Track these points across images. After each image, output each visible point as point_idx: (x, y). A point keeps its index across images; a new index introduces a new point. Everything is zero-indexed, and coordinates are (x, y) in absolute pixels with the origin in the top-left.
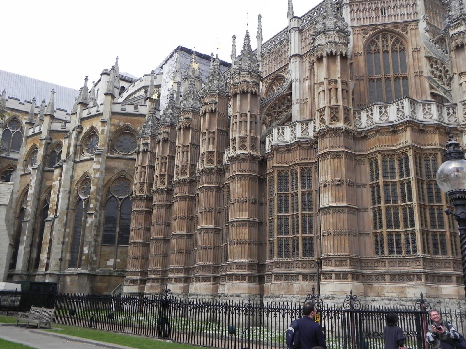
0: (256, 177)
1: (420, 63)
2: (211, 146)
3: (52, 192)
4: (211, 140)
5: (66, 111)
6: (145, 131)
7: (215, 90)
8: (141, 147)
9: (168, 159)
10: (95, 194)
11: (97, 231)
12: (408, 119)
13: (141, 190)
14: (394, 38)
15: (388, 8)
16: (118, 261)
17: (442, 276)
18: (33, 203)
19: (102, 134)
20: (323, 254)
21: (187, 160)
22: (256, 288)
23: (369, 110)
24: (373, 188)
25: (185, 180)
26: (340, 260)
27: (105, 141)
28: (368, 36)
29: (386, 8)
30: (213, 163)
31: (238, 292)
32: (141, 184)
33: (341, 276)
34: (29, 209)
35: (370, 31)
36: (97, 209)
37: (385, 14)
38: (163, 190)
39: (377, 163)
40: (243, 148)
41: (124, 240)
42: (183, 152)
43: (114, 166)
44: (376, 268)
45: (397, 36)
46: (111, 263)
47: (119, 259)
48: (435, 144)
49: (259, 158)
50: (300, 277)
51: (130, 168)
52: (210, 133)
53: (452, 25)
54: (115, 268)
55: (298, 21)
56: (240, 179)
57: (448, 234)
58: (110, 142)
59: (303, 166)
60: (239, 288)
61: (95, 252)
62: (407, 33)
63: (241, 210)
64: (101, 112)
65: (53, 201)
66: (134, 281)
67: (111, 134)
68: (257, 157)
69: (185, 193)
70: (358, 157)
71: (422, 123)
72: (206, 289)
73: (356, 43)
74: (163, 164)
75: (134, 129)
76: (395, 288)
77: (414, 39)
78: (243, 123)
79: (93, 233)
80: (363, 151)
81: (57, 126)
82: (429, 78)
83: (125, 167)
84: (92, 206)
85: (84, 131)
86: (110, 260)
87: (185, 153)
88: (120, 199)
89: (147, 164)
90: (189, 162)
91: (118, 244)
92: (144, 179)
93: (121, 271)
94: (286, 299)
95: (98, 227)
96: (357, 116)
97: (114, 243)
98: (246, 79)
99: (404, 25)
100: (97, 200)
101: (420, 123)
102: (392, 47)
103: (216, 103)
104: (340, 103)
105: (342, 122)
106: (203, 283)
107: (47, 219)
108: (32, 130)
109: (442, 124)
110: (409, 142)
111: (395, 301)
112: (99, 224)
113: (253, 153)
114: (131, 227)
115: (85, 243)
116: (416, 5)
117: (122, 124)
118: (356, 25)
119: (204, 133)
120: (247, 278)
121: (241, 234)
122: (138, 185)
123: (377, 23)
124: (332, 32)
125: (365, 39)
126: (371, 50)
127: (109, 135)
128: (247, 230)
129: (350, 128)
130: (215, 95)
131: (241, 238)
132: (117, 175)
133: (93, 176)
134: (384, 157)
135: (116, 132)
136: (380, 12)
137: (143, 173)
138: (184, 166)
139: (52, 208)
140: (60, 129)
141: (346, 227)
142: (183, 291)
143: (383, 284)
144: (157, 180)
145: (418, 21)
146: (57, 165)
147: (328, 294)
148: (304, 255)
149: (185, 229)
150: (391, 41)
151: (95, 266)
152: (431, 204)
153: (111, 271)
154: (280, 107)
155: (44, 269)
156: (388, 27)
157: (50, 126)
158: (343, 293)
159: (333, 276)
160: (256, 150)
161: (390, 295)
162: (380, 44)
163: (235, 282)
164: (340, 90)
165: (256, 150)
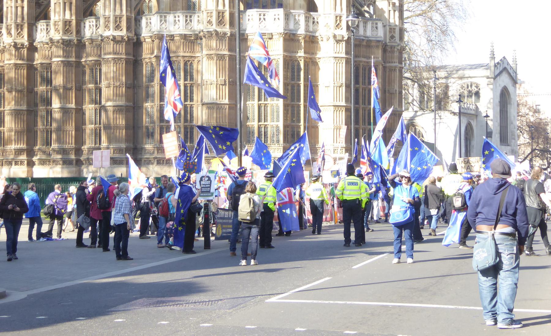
0: (131, 60)
2: (68, 12)
49: (134, 39)
59: (186, 59)
105: (228, 26)
131: (118, 123)
141: (227, 121)
152: (293, 103)
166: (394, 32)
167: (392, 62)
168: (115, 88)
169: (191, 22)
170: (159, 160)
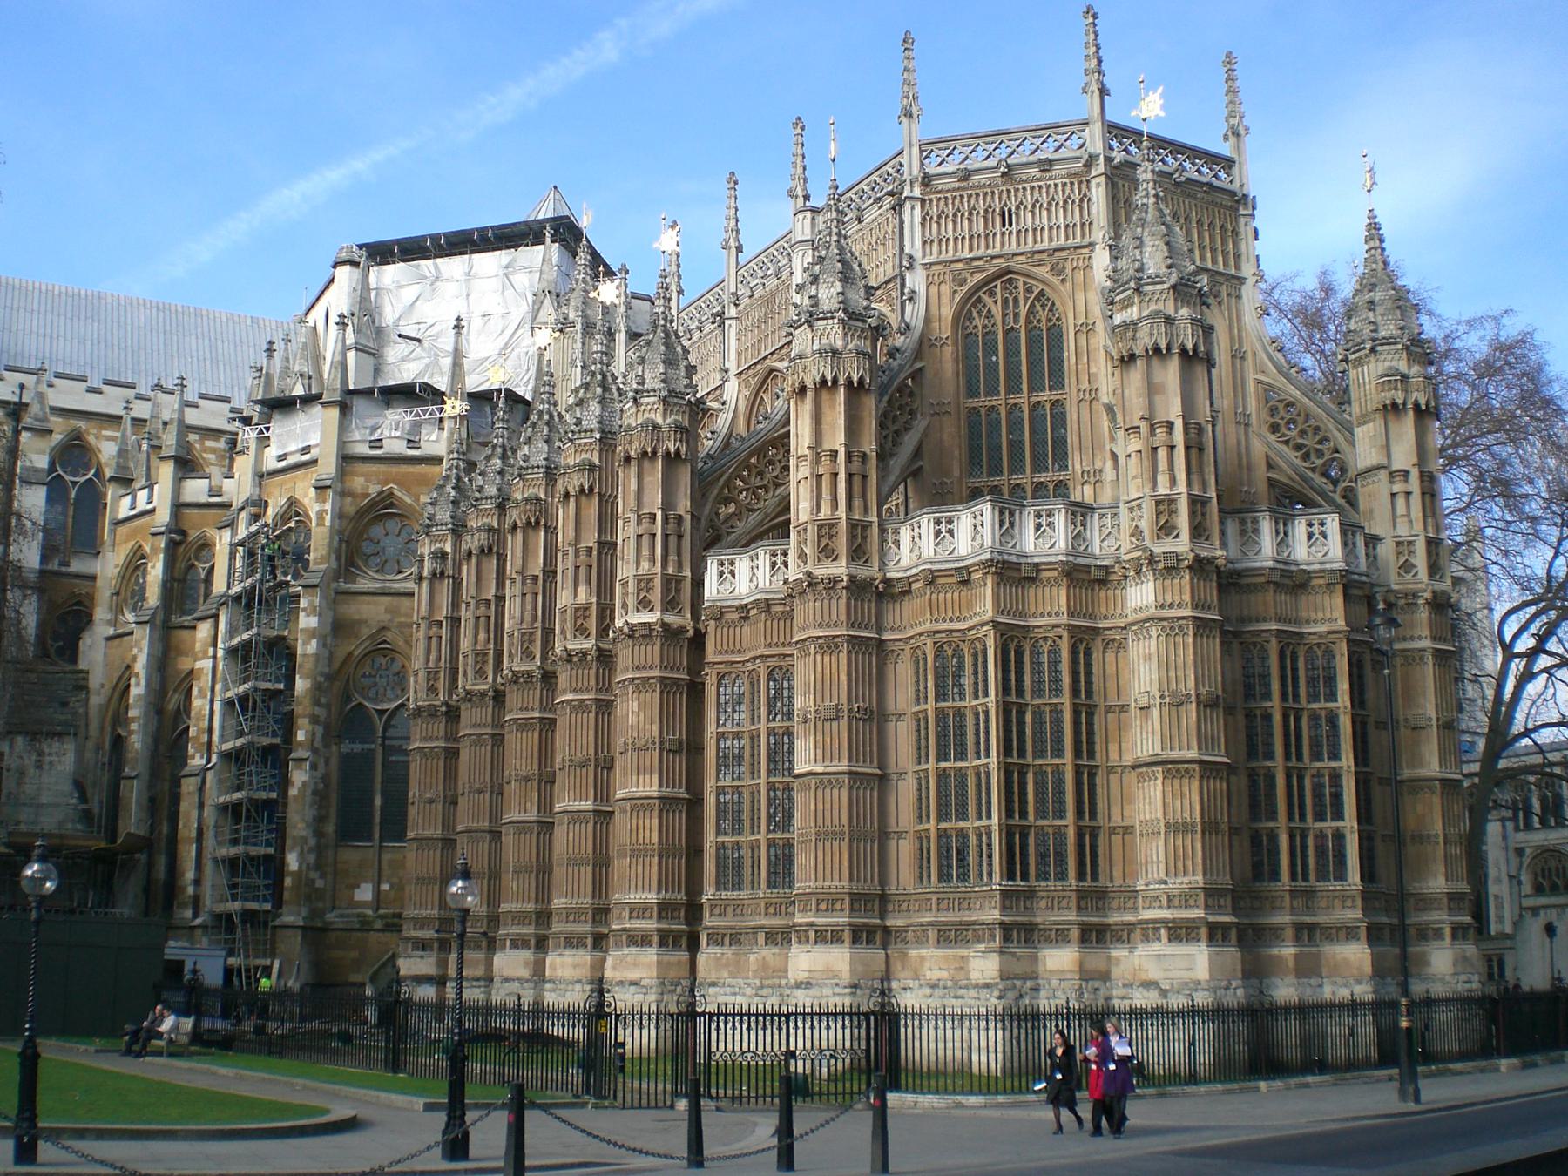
1: (1092, 364)
2: (582, 590)
3: (195, 691)
4: (582, 571)
5: (227, 400)
6: (434, 515)
7: (592, 431)
8: (426, 563)
9: (493, 607)
10: (307, 702)
11: (320, 807)
12: (988, 556)
13: (432, 689)
14: (1036, 292)
15: (1018, 208)
16: (385, 887)
17: (1051, 930)
18: (145, 725)
19: (318, 525)
20: (797, 885)
21: (535, 618)
22: (679, 962)
23: (916, 526)
24: (918, 721)
25: (529, 675)
26: (827, 901)
27: (330, 543)
28: (965, 288)
29: (1013, 209)
30: (588, 635)
31: (633, 975)
32: (429, 673)
33: (828, 936)
34: (137, 741)
35: (972, 274)
36: (318, 744)
37: (1011, 225)
38: (482, 694)
39: (925, 659)
40: (645, 608)
41: (395, 826)
42: (524, 595)
43: (357, 617)
44: (916, 915)
45: (1041, 287)
46: (365, 893)
47: (388, 881)
48: (1057, 614)
50: (761, 937)
51: (403, 619)
52: (577, 552)
53: (1118, 298)
54: (378, 909)
55: (813, 218)
56: (637, 690)
57: (1071, 832)
58: (344, 545)
59: (773, 662)
60: (636, 965)
61: (318, 866)
62: (1063, 281)
63: (641, 770)
64: (314, 453)
65: (200, 718)
66: (423, 945)
67: (345, 522)
68: (683, 630)
69: (532, 709)
70: (889, 644)
71: (1029, 561)
72: (575, 966)
73: (934, 310)
74: (482, 620)
75: (409, 501)
76: (946, 958)
77: (1080, 297)
78: (645, 540)
79: (310, 813)
80: (900, 629)
81: (196, 490)
82: (1109, 409)
83: (388, 617)
84: (301, 736)
85: (271, 512)
86: (363, 886)
87: (529, 598)
88: (381, 712)
89: (444, 613)
90: (539, 624)
91: (381, 841)
92: (439, 659)
93: (394, 916)
94: (732, 990)
95: (320, 796)
96: (891, 538)
97: (370, 838)
98: (652, 415)
99: (1055, 259)
100: (314, 720)
101: (1023, 560)
102: (1027, 317)
103: (592, 468)
104: (842, 512)
106: (568, 952)
107: (186, 771)
108: (127, 501)
109: (1081, 560)
110: (989, 615)
111: (945, 988)
112: (327, 786)
113: (670, 619)
114: (410, 794)
115: (289, 842)
116: (1089, 200)
117: (374, 490)
118: (933, 259)
119: (565, 553)
120: (656, 939)
121: (641, 831)
122: (422, 674)
123: (990, 252)
124: (830, 321)
125: (958, 298)
126: (975, 327)
127: (340, 525)
128: (655, 822)
129: (863, 572)
130: (591, 444)
132: (366, 644)
133: (299, 652)
134: (941, 646)
135: (361, 513)
136: (998, 220)
137: (434, 640)
138: (527, 637)
139: (197, 738)
140: (204, 499)
142: (535, 971)
143: (924, 952)
144: (466, 664)
145: (1092, 245)
146: (202, 609)
147: (802, 976)
148: (771, 885)
149: (535, 808)
150: (1026, 299)
151: (320, 905)
153: (365, 916)
154: (761, 474)
155: (189, 913)
156: (1014, 264)
157: (177, 491)
158: (831, 974)
159: (812, 935)
160: (680, 611)
161: (933, 975)
162: (997, 311)
163: (626, 951)
164: (842, 476)
165: (680, 611)
166: (1411, 553)
167: (1412, 638)
168: (635, 753)
169: (787, 567)
170: (713, 934)
